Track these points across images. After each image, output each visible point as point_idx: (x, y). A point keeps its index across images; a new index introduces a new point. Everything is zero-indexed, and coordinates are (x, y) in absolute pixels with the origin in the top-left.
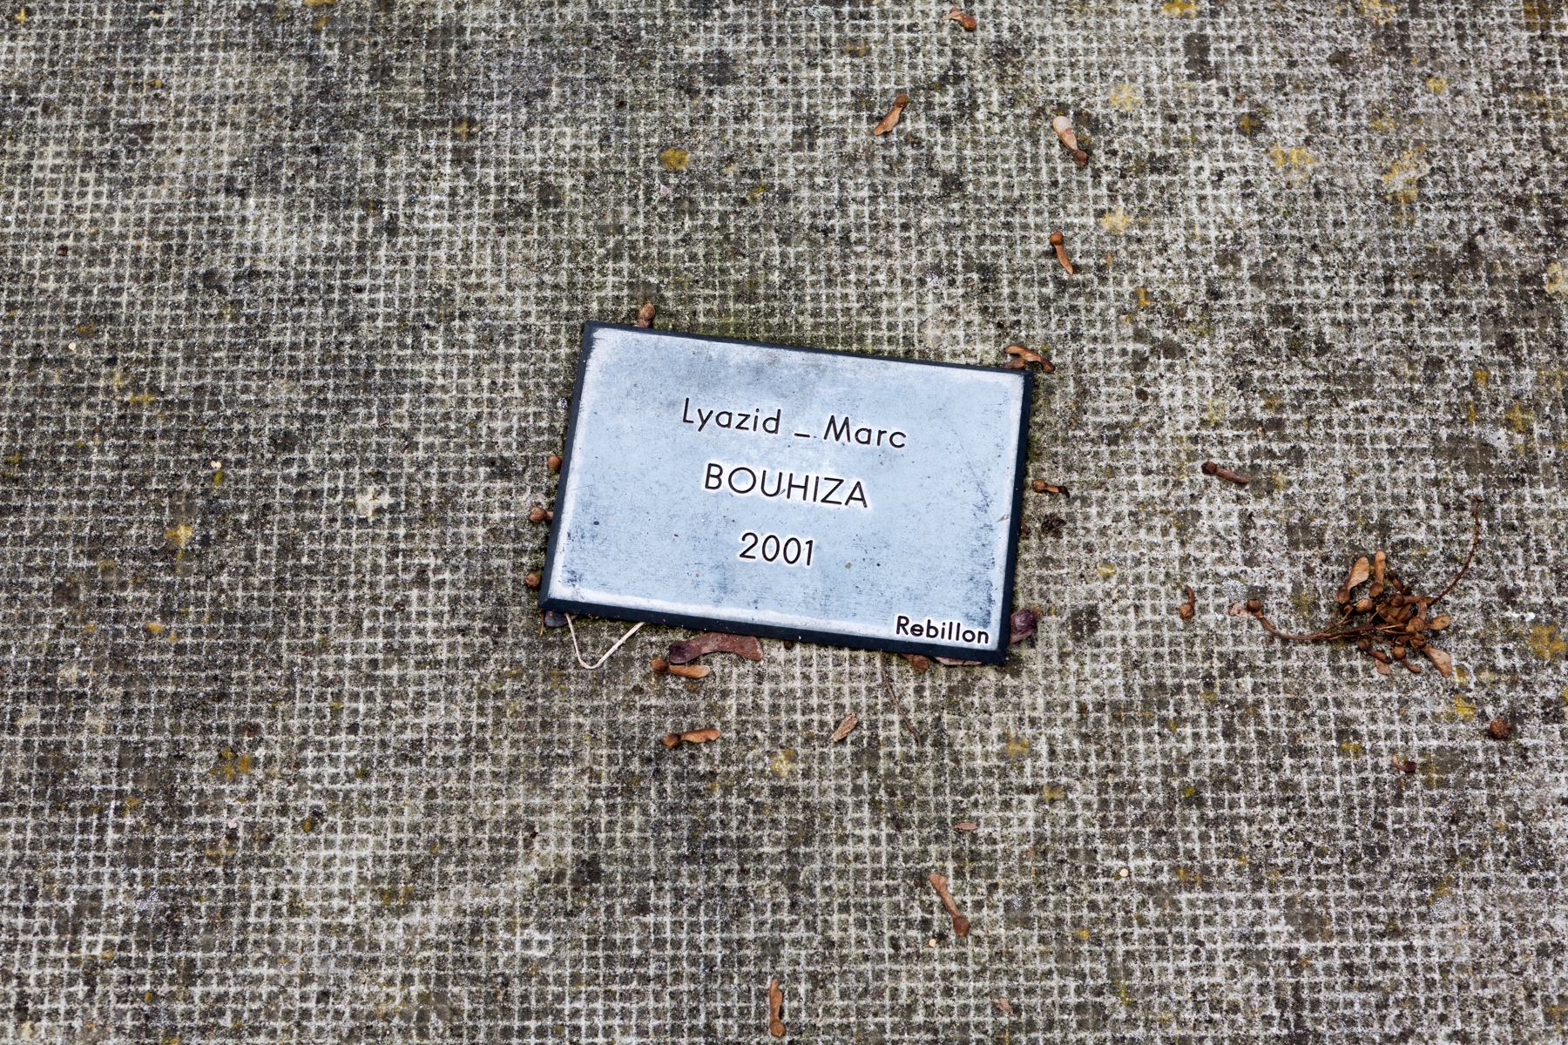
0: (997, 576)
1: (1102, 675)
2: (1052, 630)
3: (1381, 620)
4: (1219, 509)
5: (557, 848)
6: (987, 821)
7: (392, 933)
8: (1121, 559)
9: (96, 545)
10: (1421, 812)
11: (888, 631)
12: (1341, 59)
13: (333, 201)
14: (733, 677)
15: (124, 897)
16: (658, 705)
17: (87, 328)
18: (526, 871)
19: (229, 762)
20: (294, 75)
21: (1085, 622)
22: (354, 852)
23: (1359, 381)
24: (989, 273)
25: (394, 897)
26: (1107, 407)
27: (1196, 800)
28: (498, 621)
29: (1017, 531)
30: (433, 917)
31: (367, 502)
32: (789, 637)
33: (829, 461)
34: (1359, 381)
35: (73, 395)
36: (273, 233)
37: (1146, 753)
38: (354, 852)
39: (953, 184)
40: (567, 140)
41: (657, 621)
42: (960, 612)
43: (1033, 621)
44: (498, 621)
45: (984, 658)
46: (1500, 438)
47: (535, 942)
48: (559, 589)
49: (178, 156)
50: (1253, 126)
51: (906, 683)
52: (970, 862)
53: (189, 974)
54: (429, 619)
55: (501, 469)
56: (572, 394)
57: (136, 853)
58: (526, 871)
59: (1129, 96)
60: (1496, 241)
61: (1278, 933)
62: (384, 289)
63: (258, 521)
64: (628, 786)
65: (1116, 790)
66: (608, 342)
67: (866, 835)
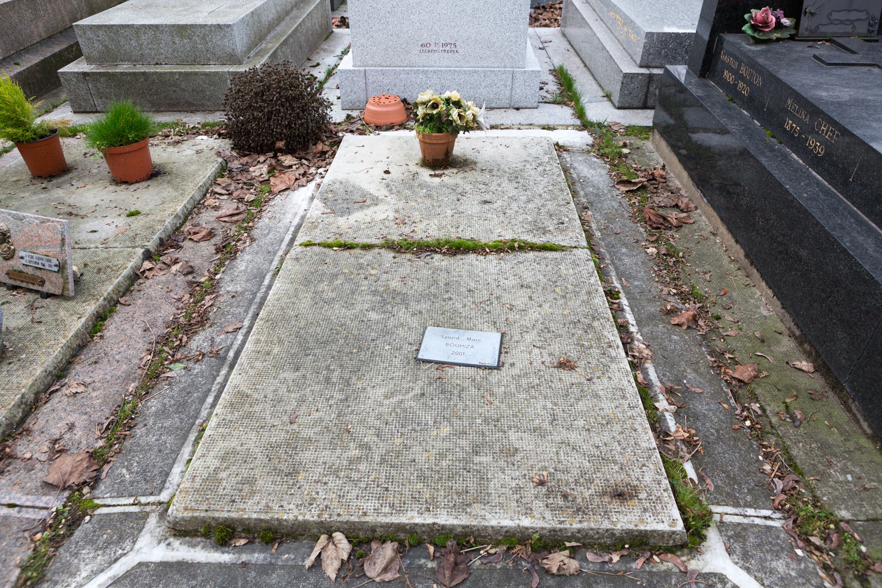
0: (497, 358)
1: (516, 371)
2: (506, 365)
3: (565, 365)
4: (536, 351)
5: (417, 391)
6: (495, 390)
7: (387, 402)
8: (519, 357)
9: (339, 352)
10: (575, 389)
11: (477, 363)
12: (555, 299)
13: (384, 312)
14: (450, 371)
15: (338, 396)
16: (437, 374)
17: (341, 326)
18: (411, 394)
19: (359, 379)
20: (379, 298)
21: (513, 365)
22: (380, 392)
23: (560, 336)
24: (495, 323)
25: (386, 397)
26: (516, 338)
27: (533, 387)
28: (408, 363)
29: (500, 353)
30: (394, 400)
31: (387, 348)
32: (460, 365)
33: (468, 343)
34: (560, 336)
35: (337, 334)
36: (373, 316)
37: (524, 382)
38: (380, 392)
39: (488, 312)
40: (424, 306)
41: (437, 362)
42: (492, 361)
43: (503, 363)
44: (408, 363)
45: (495, 368)
46: (586, 343)
47: (413, 404)
48: (420, 357)
49: (358, 307)
50: (540, 306)
51: (480, 371)
52: (492, 394)
53: (349, 406)
54: (396, 362)
55: (411, 344)
56: (423, 335)
57: (341, 390)
58: (411, 394)
59: (518, 303)
60: (583, 320)
61: (550, 405)
62: (391, 323)
63: (368, 349)
64: (431, 384)
65: (519, 386)
66: (429, 328)
67: (473, 391)
